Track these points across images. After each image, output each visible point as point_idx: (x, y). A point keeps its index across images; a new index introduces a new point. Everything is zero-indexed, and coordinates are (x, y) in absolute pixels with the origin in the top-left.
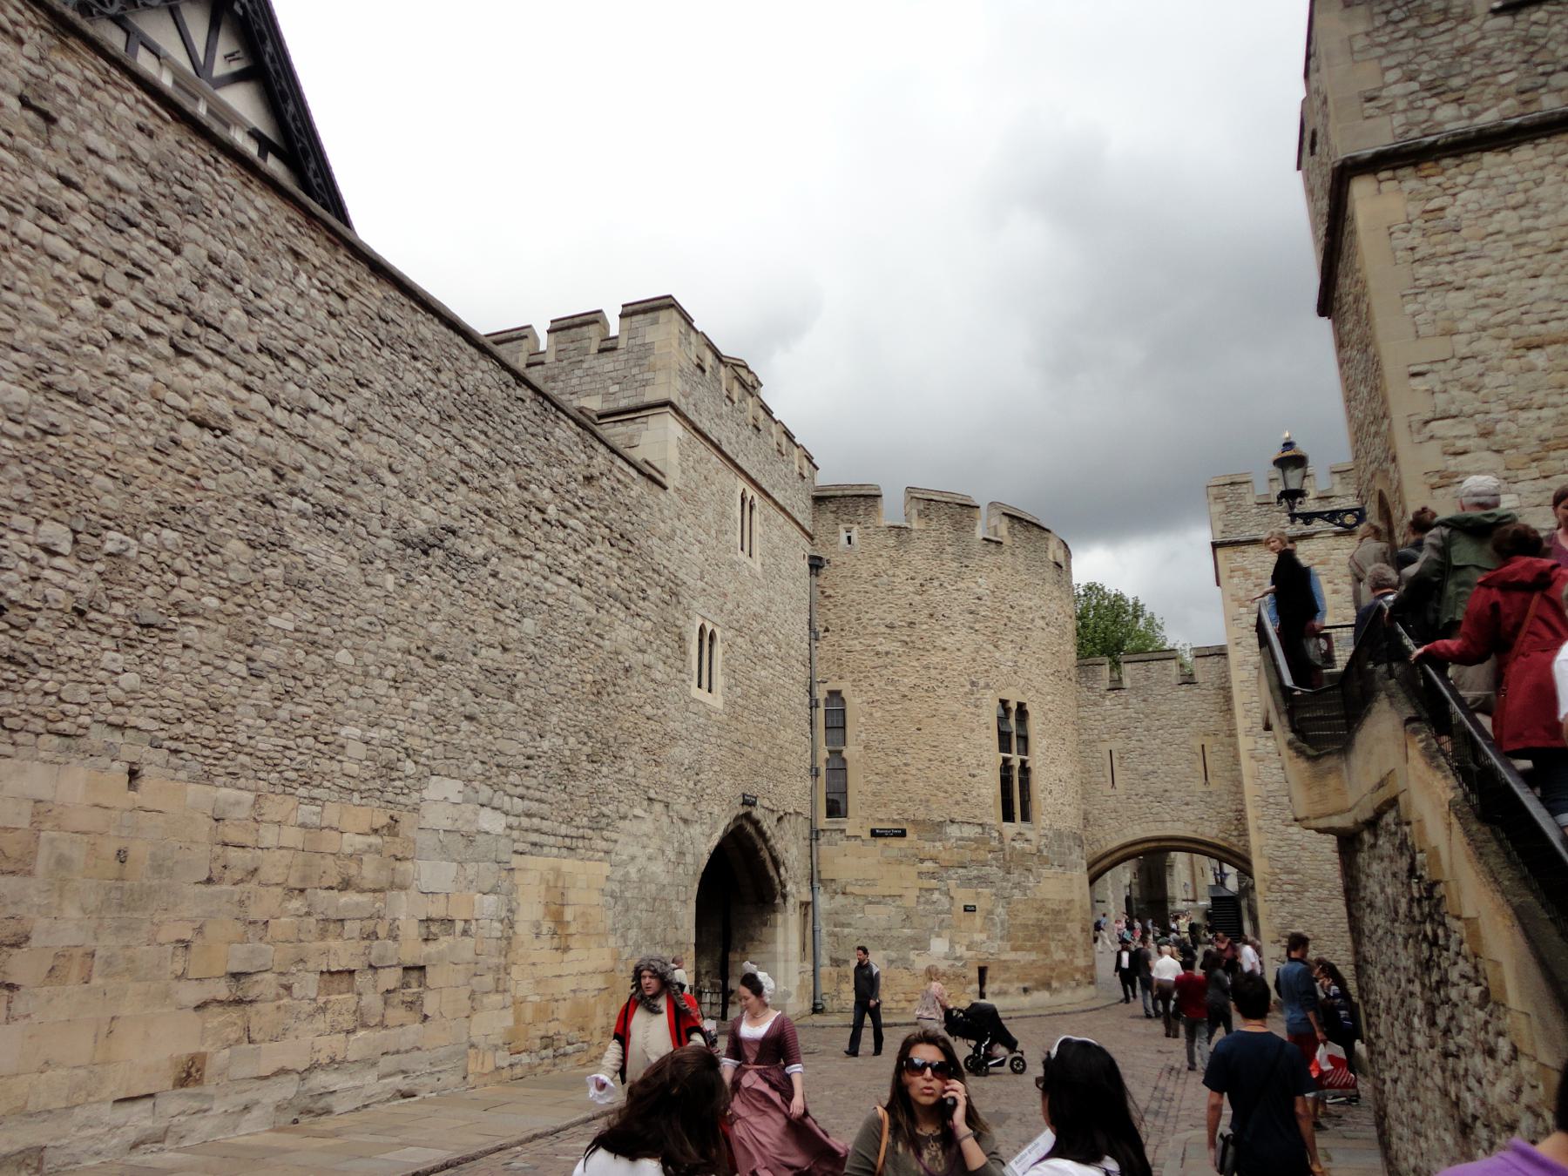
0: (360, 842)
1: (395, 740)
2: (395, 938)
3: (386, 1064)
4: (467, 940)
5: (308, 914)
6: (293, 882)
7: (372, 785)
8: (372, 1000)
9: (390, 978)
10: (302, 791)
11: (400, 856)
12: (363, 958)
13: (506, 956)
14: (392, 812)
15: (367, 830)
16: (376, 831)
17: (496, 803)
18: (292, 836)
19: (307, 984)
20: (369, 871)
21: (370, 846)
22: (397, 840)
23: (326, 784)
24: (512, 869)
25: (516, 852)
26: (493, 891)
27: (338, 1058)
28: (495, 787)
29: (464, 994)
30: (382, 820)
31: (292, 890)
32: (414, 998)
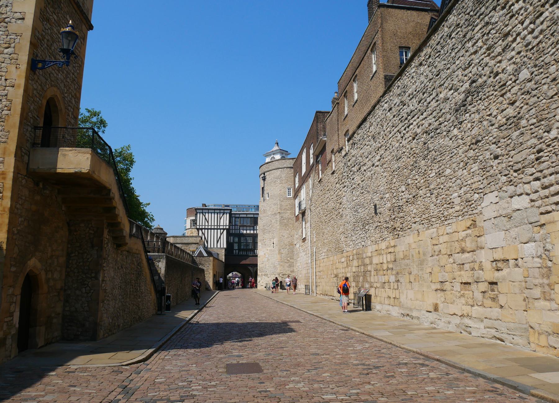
0: (463, 234)
1: (469, 189)
2: (482, 270)
3: (487, 322)
4: (517, 269)
5: (454, 263)
6: (449, 253)
7: (464, 211)
8: (479, 296)
9: (483, 286)
10: (446, 223)
11: (478, 235)
12: (472, 278)
13: (548, 277)
14: (472, 219)
15: (465, 229)
16: (469, 228)
17: (519, 190)
18: (446, 238)
19: (458, 287)
20: (469, 245)
21: (467, 235)
22: (476, 229)
23: (451, 217)
24: (544, 224)
25: (542, 214)
26: (532, 240)
27: (470, 315)
28: (515, 184)
29: (520, 298)
30: (470, 222)
31: (449, 255)
32: (495, 297)
